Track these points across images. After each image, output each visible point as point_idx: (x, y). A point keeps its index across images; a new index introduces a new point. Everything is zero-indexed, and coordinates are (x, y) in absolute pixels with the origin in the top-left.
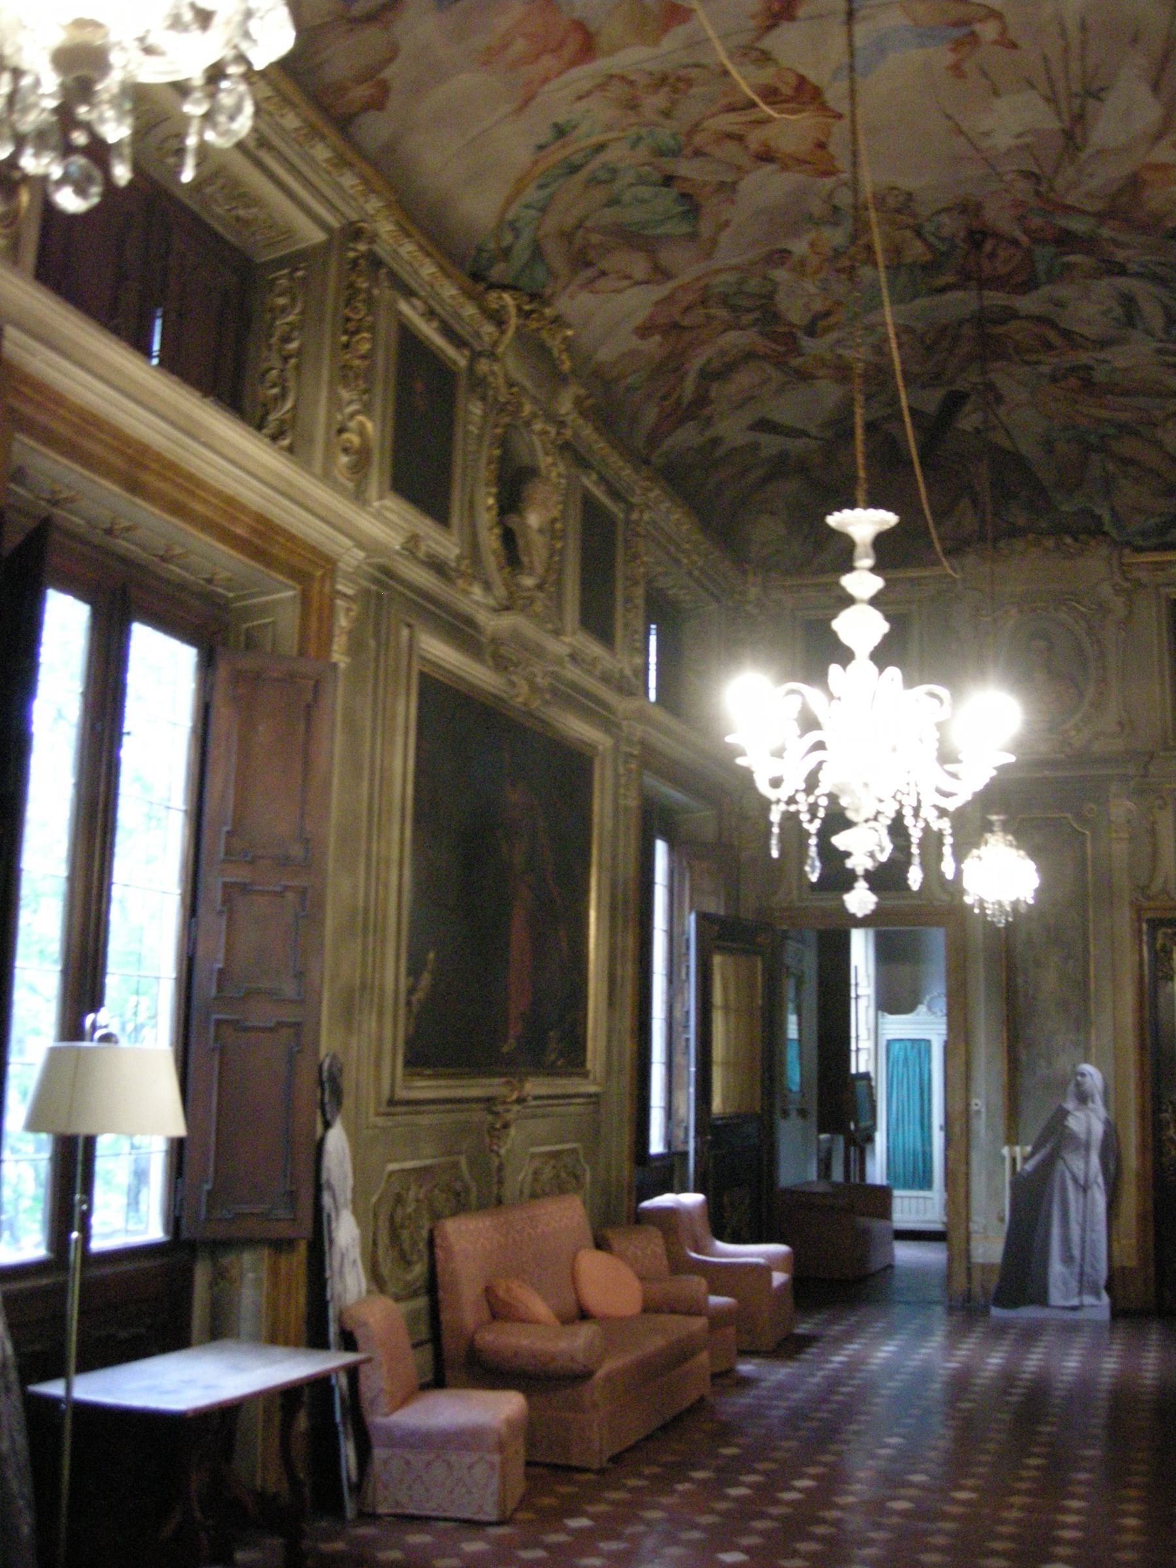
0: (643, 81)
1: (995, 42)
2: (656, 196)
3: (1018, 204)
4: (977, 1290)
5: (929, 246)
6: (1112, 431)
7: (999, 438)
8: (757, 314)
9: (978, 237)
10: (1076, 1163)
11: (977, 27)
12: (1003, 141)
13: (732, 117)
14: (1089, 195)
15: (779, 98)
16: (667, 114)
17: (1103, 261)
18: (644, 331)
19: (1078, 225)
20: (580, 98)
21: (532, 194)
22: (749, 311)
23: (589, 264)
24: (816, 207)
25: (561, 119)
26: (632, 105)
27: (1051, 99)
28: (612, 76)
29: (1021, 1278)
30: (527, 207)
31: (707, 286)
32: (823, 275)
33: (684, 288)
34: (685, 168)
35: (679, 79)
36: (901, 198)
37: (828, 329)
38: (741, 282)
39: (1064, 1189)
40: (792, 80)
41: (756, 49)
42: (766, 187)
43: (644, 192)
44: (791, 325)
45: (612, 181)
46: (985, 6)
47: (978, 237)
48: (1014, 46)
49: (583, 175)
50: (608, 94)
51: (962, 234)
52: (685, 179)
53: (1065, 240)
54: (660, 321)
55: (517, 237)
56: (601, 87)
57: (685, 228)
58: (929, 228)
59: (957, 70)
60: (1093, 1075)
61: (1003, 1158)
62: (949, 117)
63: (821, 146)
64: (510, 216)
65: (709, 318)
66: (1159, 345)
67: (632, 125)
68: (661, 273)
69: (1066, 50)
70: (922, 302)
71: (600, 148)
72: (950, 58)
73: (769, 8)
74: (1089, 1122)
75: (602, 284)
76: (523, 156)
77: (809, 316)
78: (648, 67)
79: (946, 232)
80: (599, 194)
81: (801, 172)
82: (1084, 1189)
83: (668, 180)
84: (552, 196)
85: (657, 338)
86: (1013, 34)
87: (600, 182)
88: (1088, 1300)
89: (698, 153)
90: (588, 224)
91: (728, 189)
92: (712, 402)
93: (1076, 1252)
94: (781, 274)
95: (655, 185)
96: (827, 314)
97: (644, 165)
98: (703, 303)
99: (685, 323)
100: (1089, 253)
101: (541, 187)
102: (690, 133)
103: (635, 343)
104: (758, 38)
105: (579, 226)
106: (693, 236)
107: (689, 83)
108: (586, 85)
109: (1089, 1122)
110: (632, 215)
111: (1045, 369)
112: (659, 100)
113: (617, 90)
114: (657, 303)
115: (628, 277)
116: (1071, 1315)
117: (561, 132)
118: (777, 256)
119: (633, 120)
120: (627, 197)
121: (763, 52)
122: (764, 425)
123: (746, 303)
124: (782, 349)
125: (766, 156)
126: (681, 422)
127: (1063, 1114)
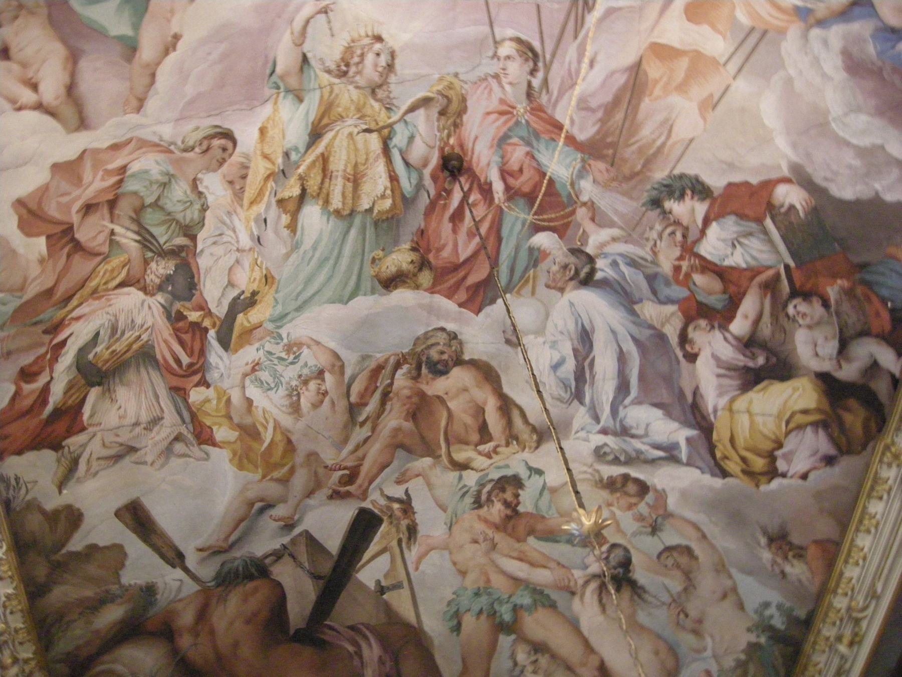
5: (393, 178)
6: (526, 600)
7: (401, 602)
9: (453, 166)
19: (559, 164)
22: (163, 254)
31: (123, 169)
32: (260, 208)
36: (383, 60)
37: (248, 334)
44: (202, 307)
47: (453, 166)
51: (434, 161)
54: (53, 211)
58: (399, 140)
66: (601, 439)
68: (73, 110)
70: (364, 304)
77: (232, 294)
79: (418, 152)
85: (40, 244)
92: (83, 429)
99: (81, 235)
100: (560, 231)
106: (130, 48)
111: (471, 479)
114: (56, 167)
115: (35, 87)
118: (217, 142)
122: (137, 517)
123: (163, 235)
124: (185, 360)
126: (36, 443)
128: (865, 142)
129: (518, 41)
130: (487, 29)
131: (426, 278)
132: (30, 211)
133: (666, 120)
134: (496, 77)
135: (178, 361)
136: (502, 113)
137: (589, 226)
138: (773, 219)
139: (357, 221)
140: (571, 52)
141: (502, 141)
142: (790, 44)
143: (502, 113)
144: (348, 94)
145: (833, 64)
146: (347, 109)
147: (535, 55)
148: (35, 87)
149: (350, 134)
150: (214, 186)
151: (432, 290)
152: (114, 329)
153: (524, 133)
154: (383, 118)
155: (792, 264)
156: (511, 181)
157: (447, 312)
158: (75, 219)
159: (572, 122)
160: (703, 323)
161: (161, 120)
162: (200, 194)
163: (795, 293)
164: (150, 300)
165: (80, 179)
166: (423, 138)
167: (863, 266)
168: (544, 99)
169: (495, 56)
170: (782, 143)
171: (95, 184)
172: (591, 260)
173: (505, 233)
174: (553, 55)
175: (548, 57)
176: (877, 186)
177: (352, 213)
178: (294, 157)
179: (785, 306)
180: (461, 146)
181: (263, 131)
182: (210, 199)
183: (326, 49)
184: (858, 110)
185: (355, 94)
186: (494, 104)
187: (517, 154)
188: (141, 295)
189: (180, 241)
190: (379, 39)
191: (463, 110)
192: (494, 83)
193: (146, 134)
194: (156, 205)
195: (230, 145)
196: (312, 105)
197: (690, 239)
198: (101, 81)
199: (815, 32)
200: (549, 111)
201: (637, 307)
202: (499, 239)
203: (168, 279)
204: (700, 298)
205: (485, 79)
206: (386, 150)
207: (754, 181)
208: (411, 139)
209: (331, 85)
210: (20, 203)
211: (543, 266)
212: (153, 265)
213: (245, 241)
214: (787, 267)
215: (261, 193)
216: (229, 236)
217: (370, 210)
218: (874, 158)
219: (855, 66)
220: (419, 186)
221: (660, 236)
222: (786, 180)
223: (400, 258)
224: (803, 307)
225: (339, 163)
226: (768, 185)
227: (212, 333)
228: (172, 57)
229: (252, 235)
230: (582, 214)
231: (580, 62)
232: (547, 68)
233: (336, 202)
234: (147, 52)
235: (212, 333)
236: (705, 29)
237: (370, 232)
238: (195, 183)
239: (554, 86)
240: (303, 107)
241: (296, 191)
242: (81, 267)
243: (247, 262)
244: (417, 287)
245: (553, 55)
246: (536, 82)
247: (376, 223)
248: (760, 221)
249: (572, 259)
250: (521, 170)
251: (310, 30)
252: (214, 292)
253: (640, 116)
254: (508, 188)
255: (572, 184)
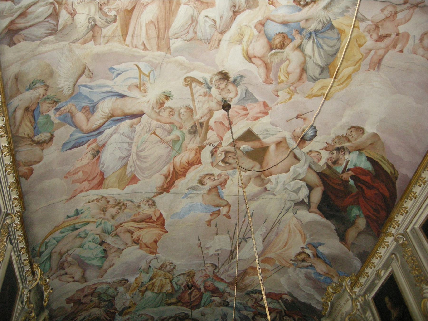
0: (112, 202)
1: (225, 215)
2: (96, 247)
3: (207, 276)
5: (172, 287)
8: (107, 303)
9: (190, 287)
11: (221, 208)
12: (212, 252)
13: (133, 224)
14: (229, 276)
15: (152, 221)
16: (113, 217)
17: (223, 301)
18: (69, 301)
19: (221, 286)
20: (89, 202)
21: (57, 234)
22: (105, 301)
23: (63, 268)
24: (143, 265)
25: (79, 208)
26: (104, 210)
27: (232, 239)
28: (103, 197)
30: (54, 238)
31: (96, 288)
32: (134, 292)
33: (89, 287)
34: (109, 240)
35: (123, 205)
36: (172, 267)
38: (108, 289)
40: (158, 215)
41: (152, 200)
42: (132, 254)
43: (92, 245)
44: (116, 309)
45: (85, 238)
46: (227, 202)
47: (190, 287)
48: (229, 217)
49: (76, 232)
50: (99, 203)
51: (185, 284)
52: (109, 244)
53: (215, 291)
54: (76, 298)
55: (46, 249)
56: (98, 200)
57: (99, 264)
58: (175, 280)
59: (209, 223)
62: (199, 240)
63: (156, 242)
64: (47, 240)
65: (91, 301)
67: (100, 218)
69: (244, 222)
70: (161, 308)
71: (87, 223)
72: (209, 218)
73: (163, 186)
75: (63, 277)
76: (61, 218)
77: (123, 307)
78: (116, 197)
79: (180, 282)
80: (78, 242)
81: (145, 251)
83: (102, 243)
84: (63, 238)
85: (72, 305)
86: (230, 214)
87: (81, 237)
89: (116, 235)
90: (70, 252)
91: (120, 251)
94: (121, 289)
95: (97, 244)
96: (129, 307)
97: (97, 235)
98: (92, 294)
100: (220, 297)
101: (62, 232)
102: (117, 227)
103: (64, 304)
104: (154, 197)
105: (67, 252)
107: (126, 207)
108: (94, 198)
110: (85, 253)
112: (113, 211)
113: (103, 202)
114: (78, 291)
115: (73, 278)
117: (77, 213)
119: (102, 216)
120: (86, 246)
121: (154, 202)
123: (105, 298)
124: (109, 318)
125: (137, 242)
128: (309, 292)
129: (212, 264)
130: (203, 262)
131: (180, 304)
132: (70, 300)
133: (253, 280)
134: (205, 270)
135: (107, 319)
136: (205, 276)
137: (228, 297)
138: (281, 300)
139: (161, 294)
140: (227, 266)
141: (205, 281)
142: (291, 270)
143: (205, 276)
144: (161, 272)
145: (302, 276)
146: (161, 275)
147: (216, 266)
148: (73, 278)
149: (161, 279)
150: (121, 289)
151: (181, 306)
152: (90, 315)
153: (211, 280)
154: (171, 276)
155: (286, 310)
156: (206, 288)
157: (185, 310)
158: (82, 298)
159: (225, 279)
160: (259, 316)
161: (108, 278)
162: (117, 290)
163: (286, 315)
164: (101, 309)
165: (84, 291)
166: (183, 280)
167: (304, 316)
168: (218, 274)
169: (205, 266)
170: (286, 287)
171: (87, 291)
172: (228, 302)
173: (204, 297)
174: (222, 267)
175: (220, 267)
176: (311, 302)
177: (160, 293)
178: (144, 283)
179: (283, 316)
180: (193, 281)
181: (136, 279)
182: (120, 291)
183: (155, 264)
184: (308, 286)
185: (163, 272)
186: (203, 274)
187: (209, 284)
188: (98, 309)
189: (111, 298)
190: (172, 263)
191: (194, 275)
192: (204, 271)
193: (104, 281)
194: (105, 293)
195: (127, 282)
196: (151, 275)
197: (257, 301)
198: (91, 274)
199: (298, 269)
200: (219, 276)
201: (241, 311)
202: (202, 298)
203: (106, 305)
204: (259, 311)
205: (201, 270)
206: (171, 282)
207: (277, 293)
208: (179, 280)
209: (157, 271)
210: (67, 299)
211: (214, 303)
212: (102, 303)
213: (128, 297)
214: (284, 310)
215: (134, 289)
216: (124, 297)
217: (166, 292)
218: (310, 296)
219: (308, 277)
220: (180, 288)
221: (249, 300)
222: (285, 294)
223: (174, 300)
224: (288, 318)
225: (158, 284)
226: (281, 295)
227: (117, 314)
228: (112, 268)
229: (131, 296)
230: (226, 294)
231: (229, 268)
232: (219, 269)
233: (156, 290)
234: (105, 267)
235: (117, 314)
236: (266, 264)
237: (165, 296)
238: (116, 288)
239: (221, 272)
240: (148, 275)
241: (145, 289)
242: (81, 307)
243: (129, 302)
244: (177, 305)
245: (222, 267)
246: (216, 271)
247: (167, 295)
248: (278, 300)
249: (223, 302)
250: (210, 286)
251: (152, 261)
252: (119, 306)
253: (245, 279)
254: (205, 289)
255: (224, 289)
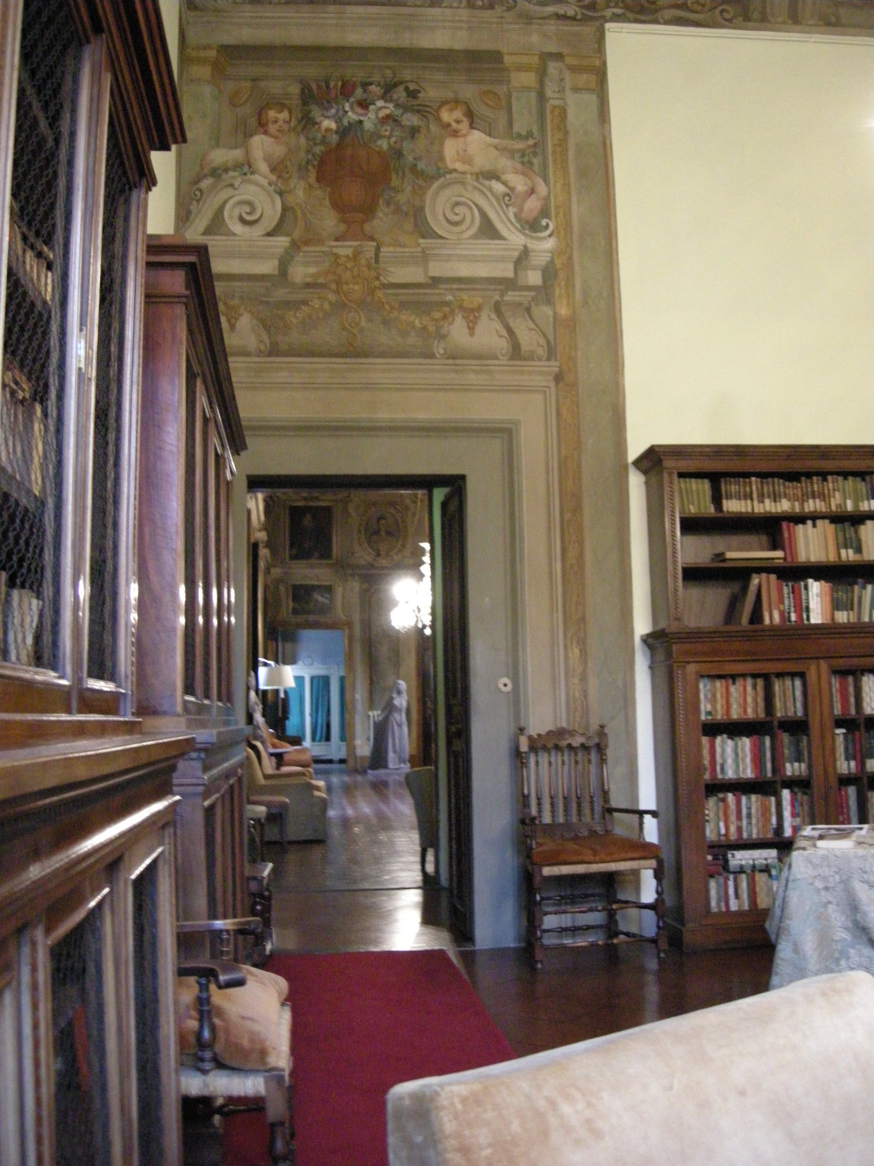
4: (359, 766)
10: (396, 716)
29: (378, 759)
39: (393, 726)
60: (403, 685)
61: (369, 716)
74: (401, 702)
82: (400, 725)
88: (402, 765)
93: (398, 748)
109: (401, 702)
116: (396, 771)
127: (392, 698)
